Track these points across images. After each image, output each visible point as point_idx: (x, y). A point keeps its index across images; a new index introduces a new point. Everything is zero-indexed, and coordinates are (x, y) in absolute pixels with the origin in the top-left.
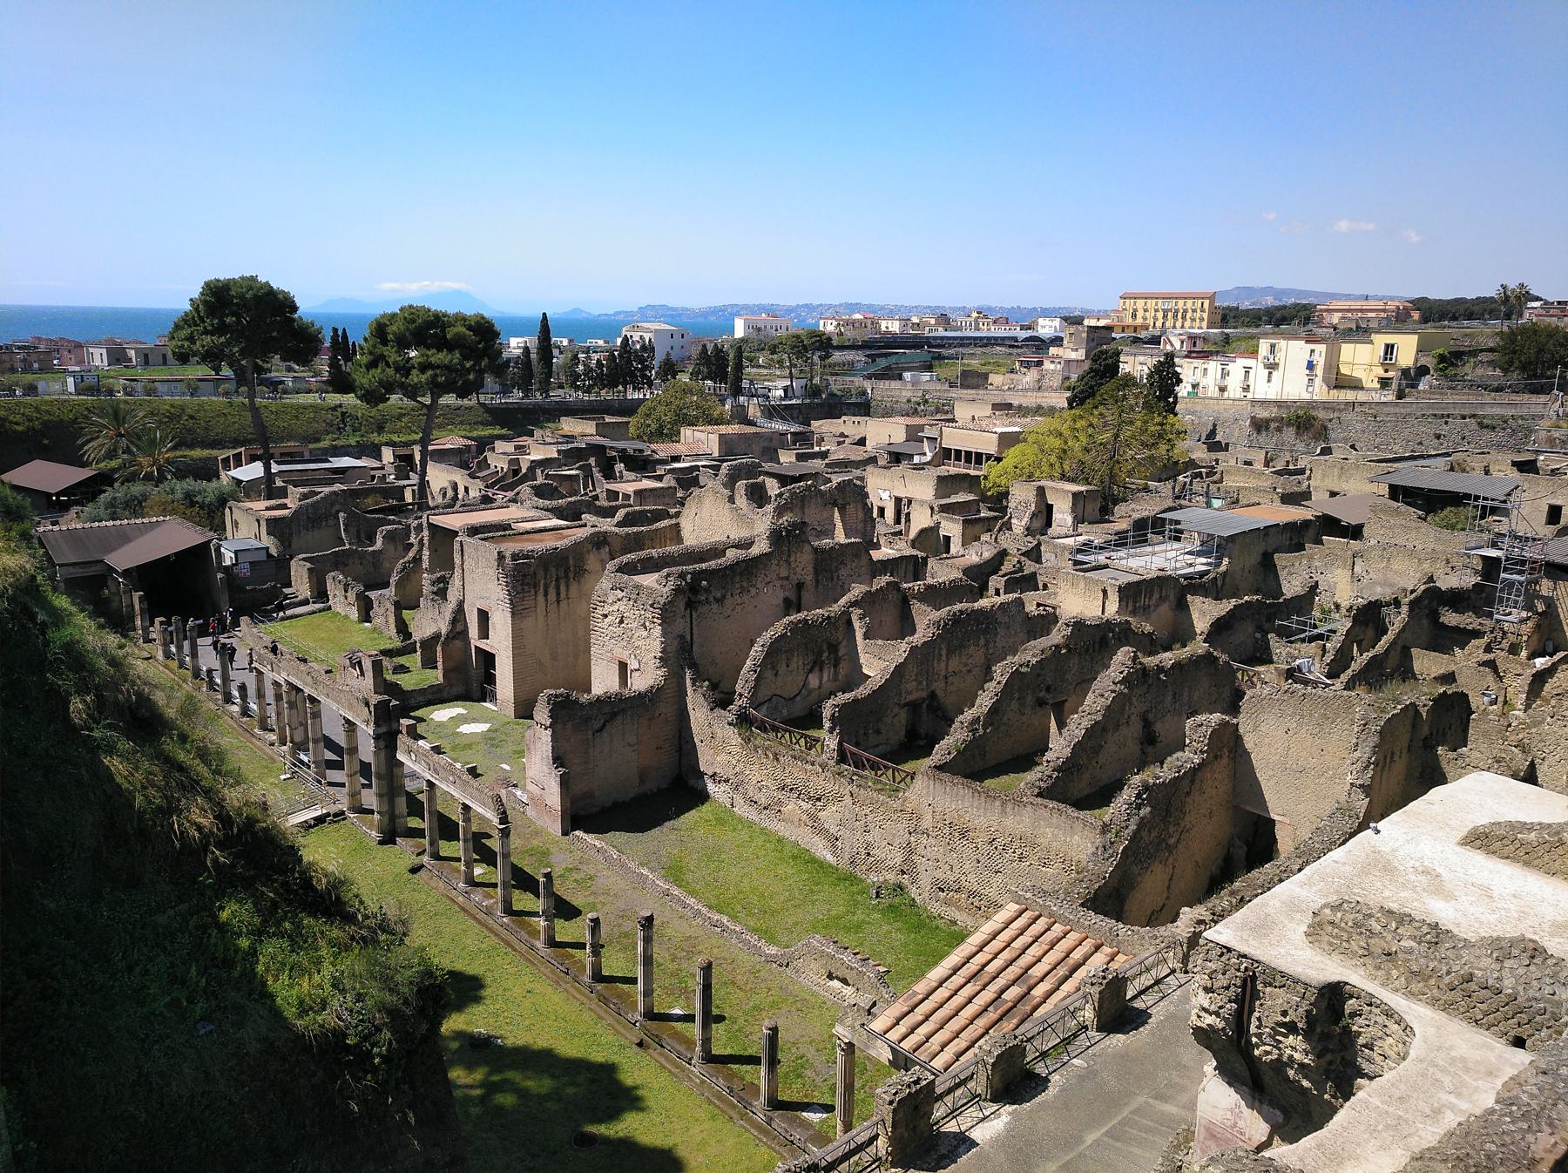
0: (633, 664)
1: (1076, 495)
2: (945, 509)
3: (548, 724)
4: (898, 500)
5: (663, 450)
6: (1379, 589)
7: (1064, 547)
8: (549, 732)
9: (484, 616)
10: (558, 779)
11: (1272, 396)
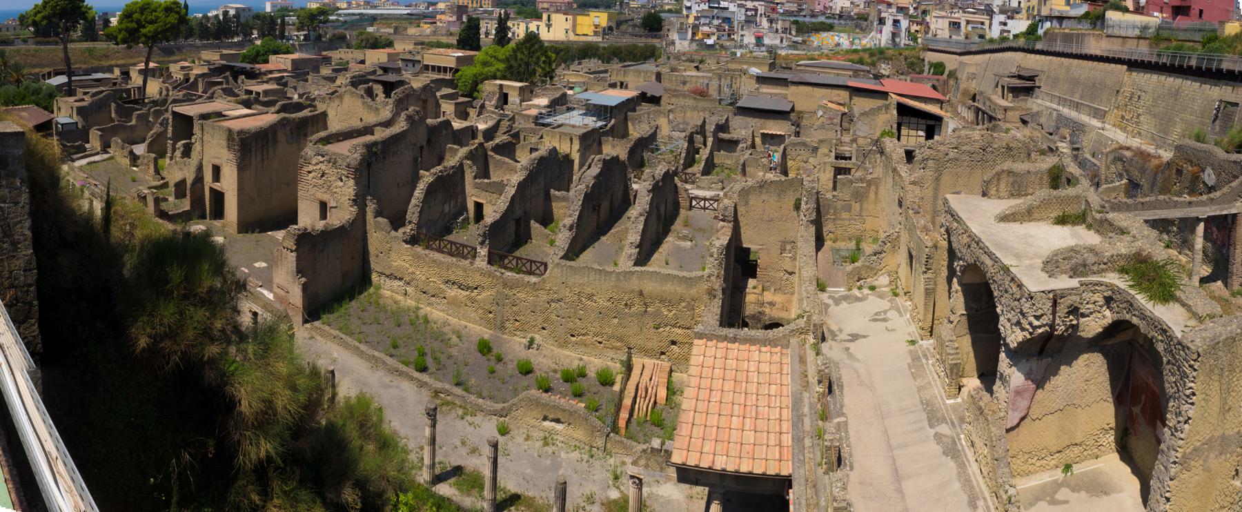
5: (264, 67)
8: (294, 254)
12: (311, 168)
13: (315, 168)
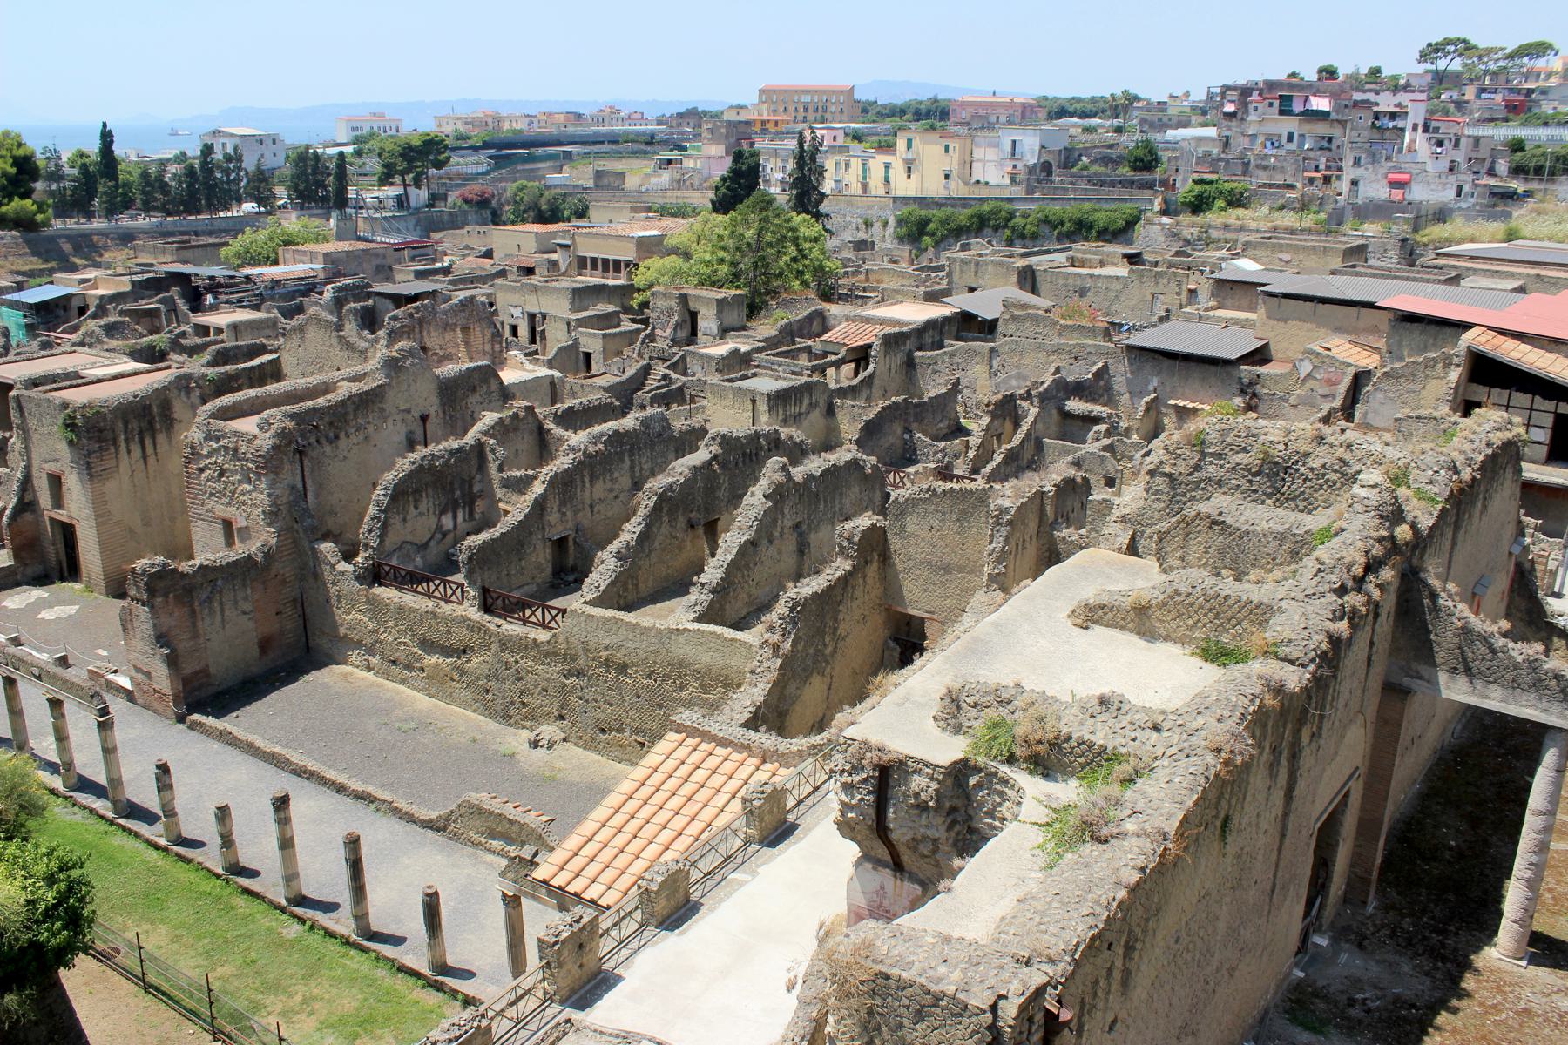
4: (532, 316)
9: (56, 481)
11: (912, 194)
13: (207, 462)
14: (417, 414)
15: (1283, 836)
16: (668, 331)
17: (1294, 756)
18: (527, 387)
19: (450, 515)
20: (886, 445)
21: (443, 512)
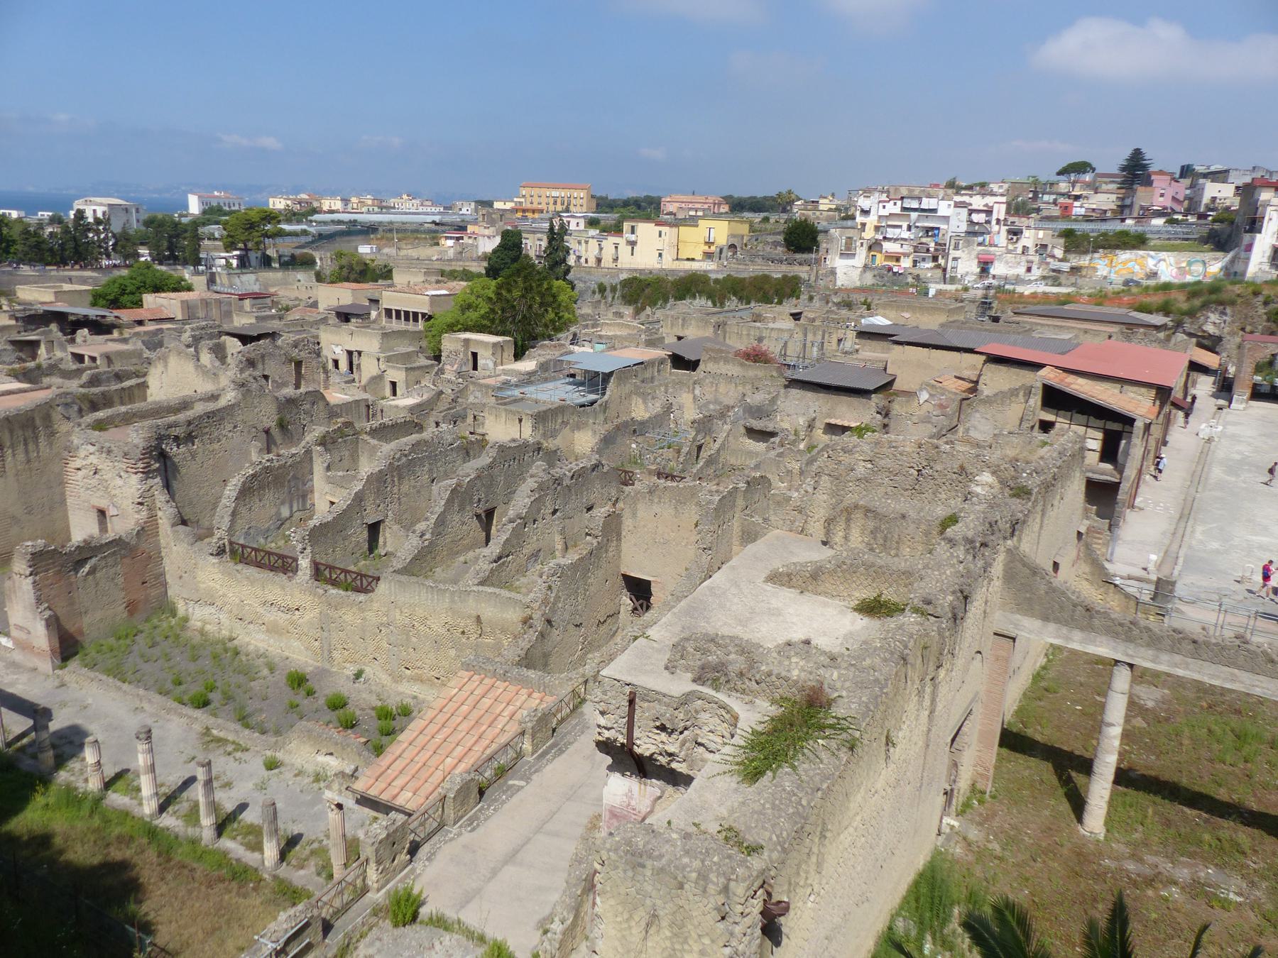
0: (111, 511)
1: (495, 345)
2: (389, 359)
3: (28, 571)
4: (350, 353)
5: (126, 315)
6: (712, 407)
7: (487, 386)
10: (43, 623)
12: (78, 463)
14: (260, 428)
15: (928, 746)
16: (456, 366)
17: (935, 687)
18: (346, 407)
19: (287, 506)
20: (619, 453)
21: (283, 503)
